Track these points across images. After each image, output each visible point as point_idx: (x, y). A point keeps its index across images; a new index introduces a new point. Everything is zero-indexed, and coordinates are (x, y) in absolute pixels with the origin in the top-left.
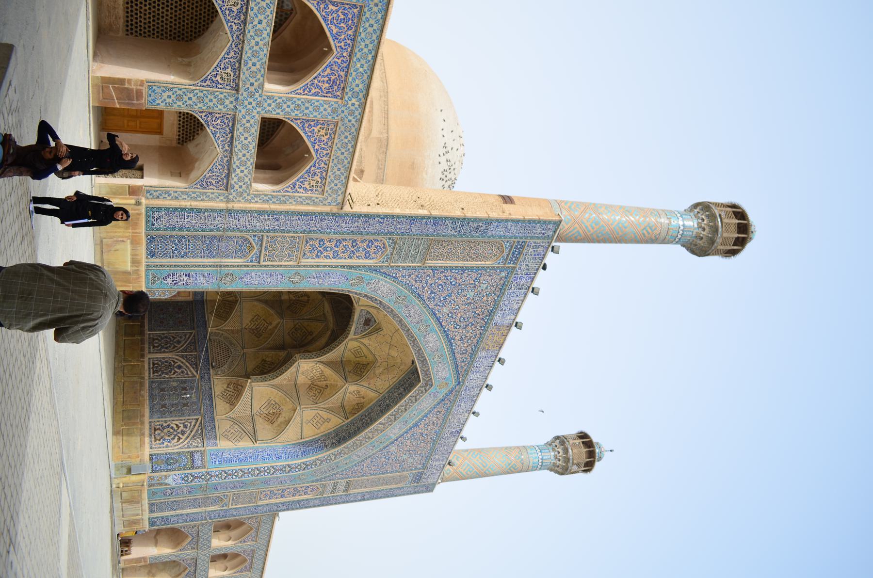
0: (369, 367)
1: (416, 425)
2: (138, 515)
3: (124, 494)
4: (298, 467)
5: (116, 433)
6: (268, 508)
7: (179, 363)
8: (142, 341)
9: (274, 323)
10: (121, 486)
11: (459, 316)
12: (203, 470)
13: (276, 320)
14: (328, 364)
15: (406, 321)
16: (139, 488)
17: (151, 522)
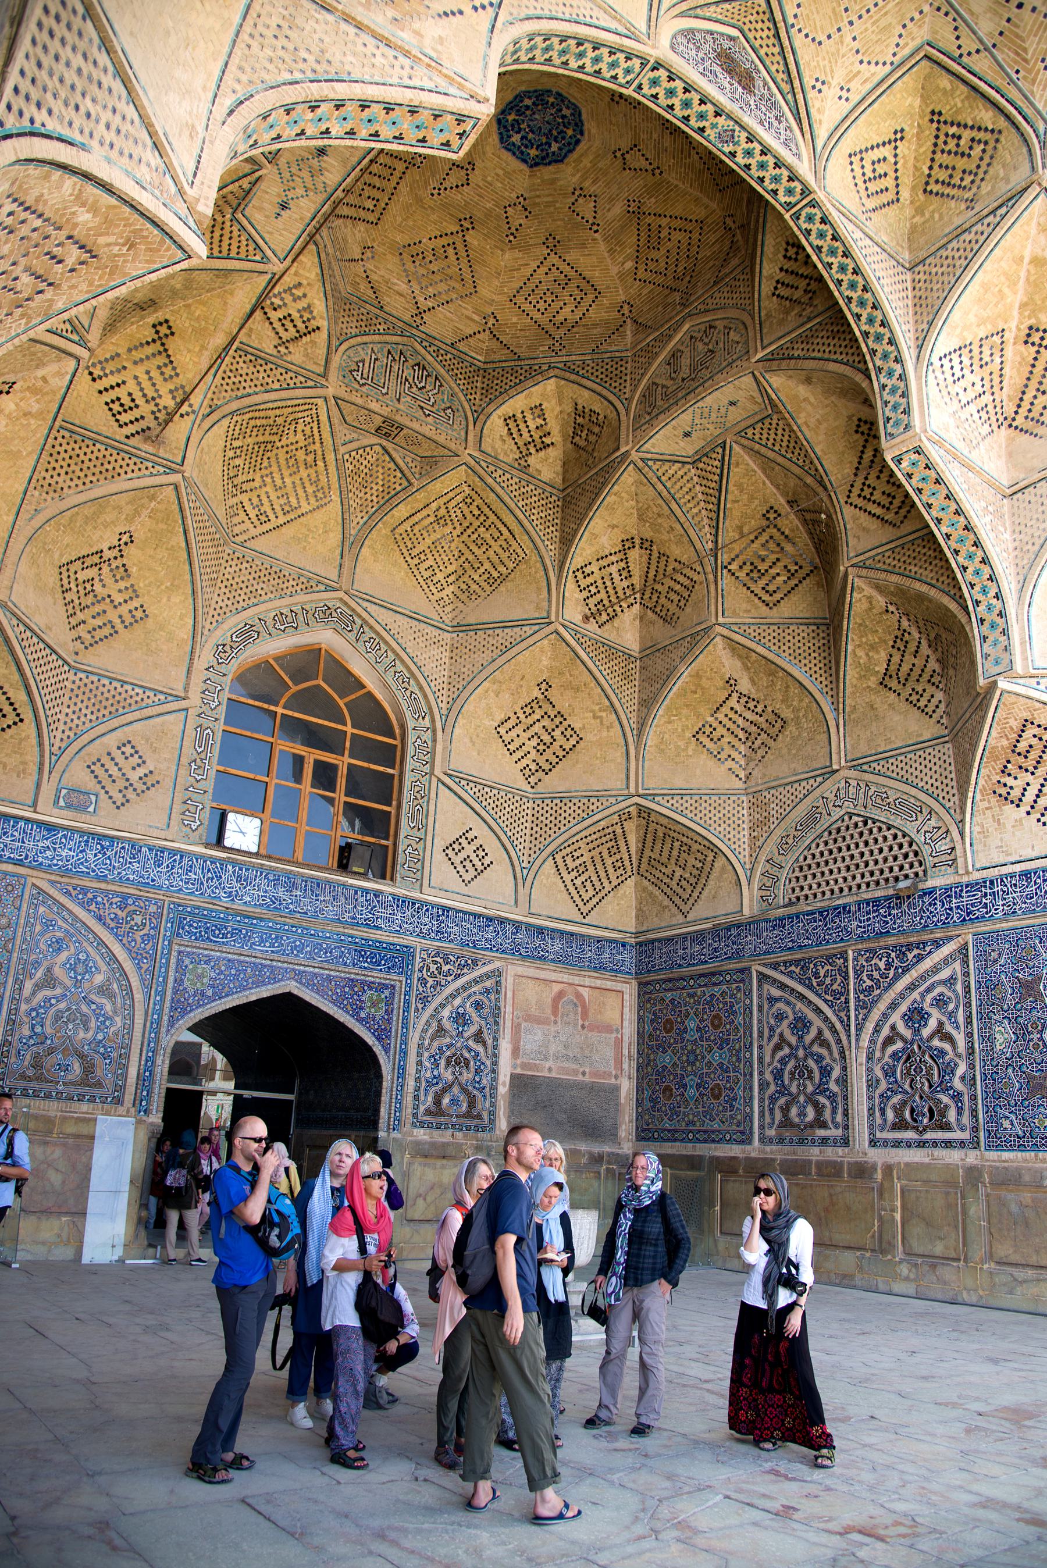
7: (896, 1018)
9: (731, 666)
14: (929, 311)
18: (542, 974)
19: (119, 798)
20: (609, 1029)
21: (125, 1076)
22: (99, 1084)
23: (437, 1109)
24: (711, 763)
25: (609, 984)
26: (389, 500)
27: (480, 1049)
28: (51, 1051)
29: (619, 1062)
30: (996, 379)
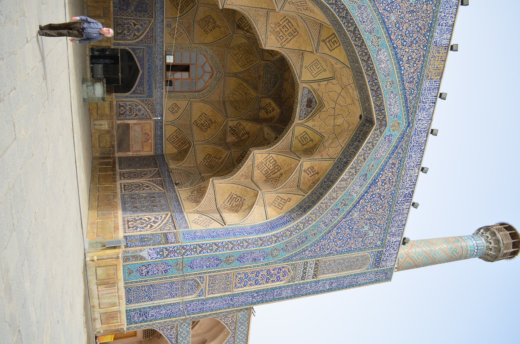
0: (317, 146)
1: (374, 182)
2: (114, 305)
3: (100, 271)
4: (269, 240)
5: (90, 208)
6: (242, 299)
7: (147, 184)
8: (114, 175)
9: (223, 157)
10: (95, 258)
11: (405, 27)
12: (178, 244)
13: (225, 154)
14: (281, 152)
15: (361, 27)
16: (114, 262)
17: (130, 320)
18: (152, 130)
19: (171, 33)
20: (143, 148)
21: (119, 40)
22: (117, 36)
23: (120, 106)
24: (203, 158)
25: (153, 148)
26: (247, 81)
27: (134, 115)
28: (122, 26)
29: (136, 151)
30: (273, 172)
